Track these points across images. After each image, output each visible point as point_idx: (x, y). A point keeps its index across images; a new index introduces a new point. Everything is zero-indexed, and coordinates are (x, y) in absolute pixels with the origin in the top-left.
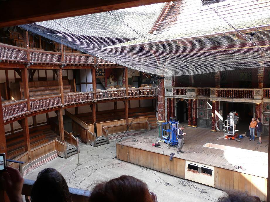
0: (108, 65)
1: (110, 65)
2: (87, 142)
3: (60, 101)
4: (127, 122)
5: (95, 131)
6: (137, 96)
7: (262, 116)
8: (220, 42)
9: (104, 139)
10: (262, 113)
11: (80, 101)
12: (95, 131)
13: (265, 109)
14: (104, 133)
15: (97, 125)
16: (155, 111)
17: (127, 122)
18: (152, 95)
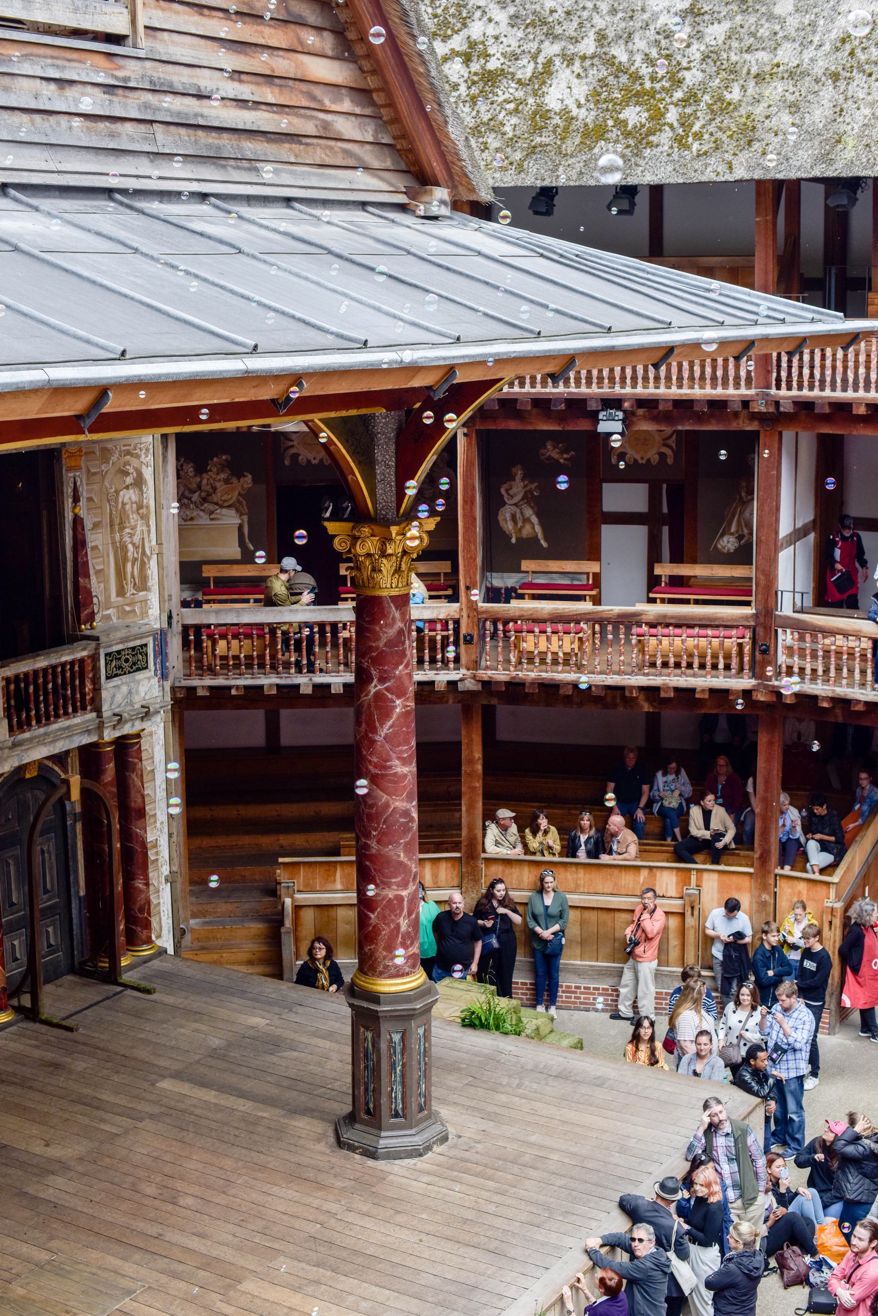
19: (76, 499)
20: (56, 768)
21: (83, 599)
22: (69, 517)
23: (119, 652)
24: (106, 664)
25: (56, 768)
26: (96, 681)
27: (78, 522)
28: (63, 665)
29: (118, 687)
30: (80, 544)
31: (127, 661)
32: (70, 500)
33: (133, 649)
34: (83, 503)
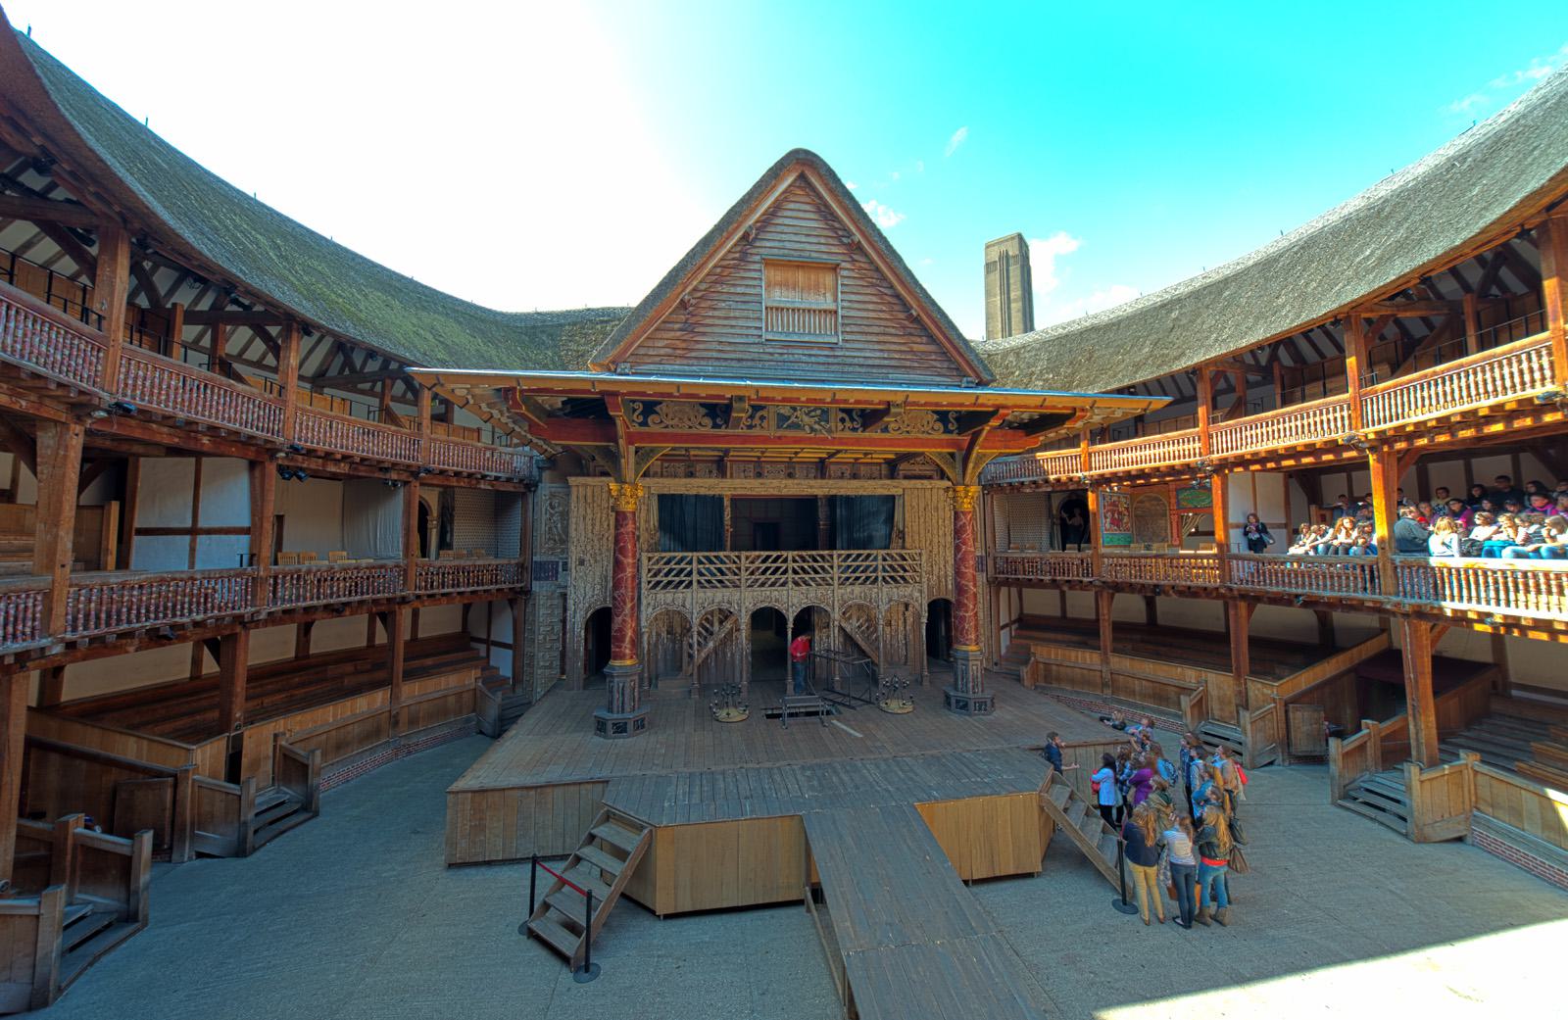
0: (345, 457)
1: (358, 460)
2: (171, 848)
3: (34, 619)
4: (394, 697)
5: (233, 772)
6: (451, 590)
8: (817, 427)
9: (283, 803)
11: (174, 616)
12: (233, 772)
14: (292, 767)
15: (246, 735)
16: (482, 648)
17: (394, 697)
18: (503, 586)
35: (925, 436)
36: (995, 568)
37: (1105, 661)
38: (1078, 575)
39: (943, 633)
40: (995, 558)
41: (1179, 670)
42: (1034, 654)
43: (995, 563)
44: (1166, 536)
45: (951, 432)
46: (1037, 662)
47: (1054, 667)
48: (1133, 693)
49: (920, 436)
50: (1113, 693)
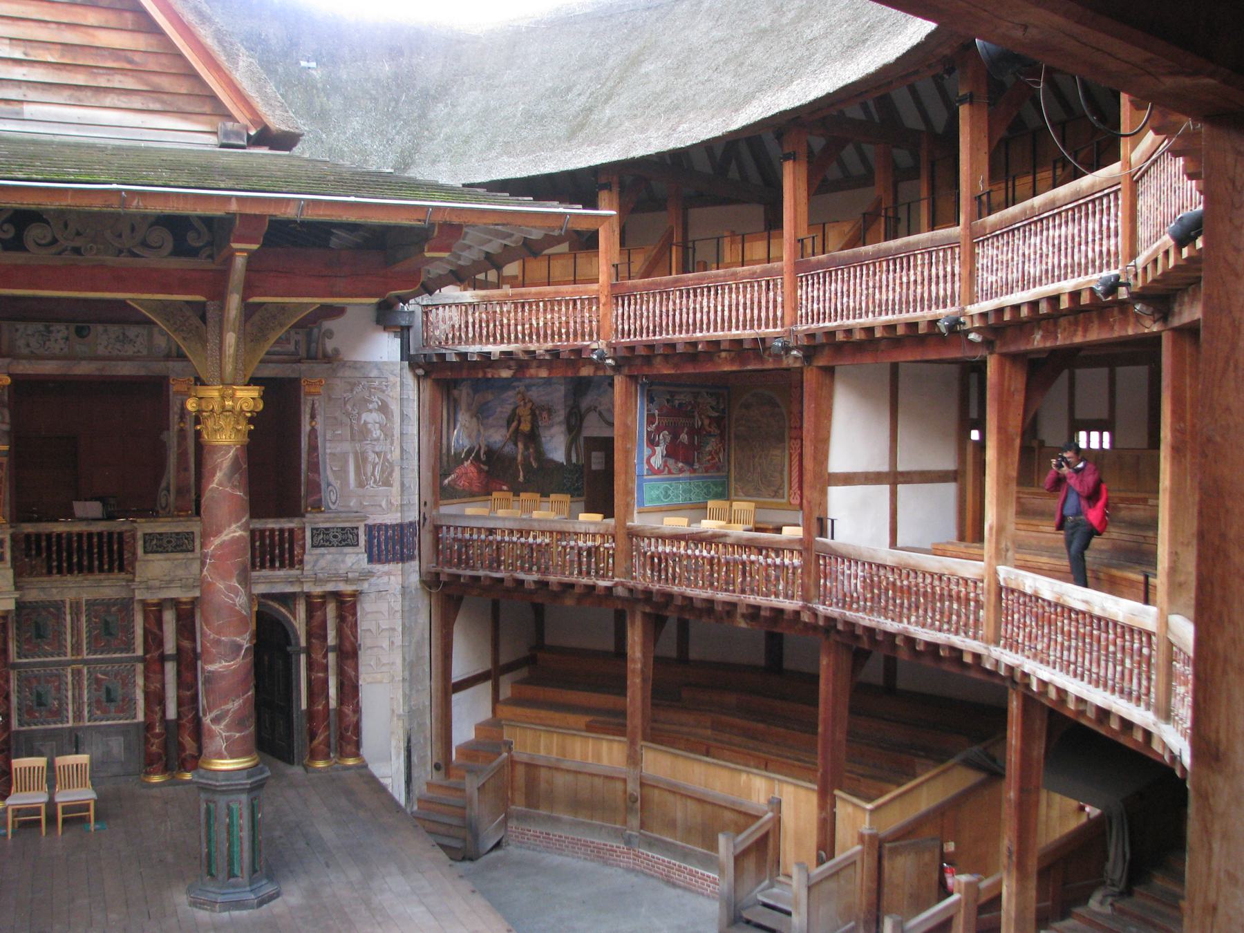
7: (13, 685)
10: (14, 666)
13: (28, 640)
19: (313, 417)
20: (283, 610)
21: (315, 487)
22: (306, 427)
23: (327, 529)
24: (312, 537)
25: (283, 610)
26: (303, 547)
27: (313, 431)
28: (272, 531)
29: (323, 555)
30: (313, 448)
31: (335, 537)
32: (308, 417)
33: (343, 529)
34: (319, 419)
35: (125, 260)
36: (437, 552)
37: (634, 759)
38: (588, 573)
39: (304, 706)
40: (437, 529)
41: (744, 777)
42: (509, 745)
43: (437, 540)
44: (781, 487)
45: (193, 253)
46: (513, 763)
47: (543, 773)
48: (671, 825)
49: (110, 260)
50: (643, 825)
